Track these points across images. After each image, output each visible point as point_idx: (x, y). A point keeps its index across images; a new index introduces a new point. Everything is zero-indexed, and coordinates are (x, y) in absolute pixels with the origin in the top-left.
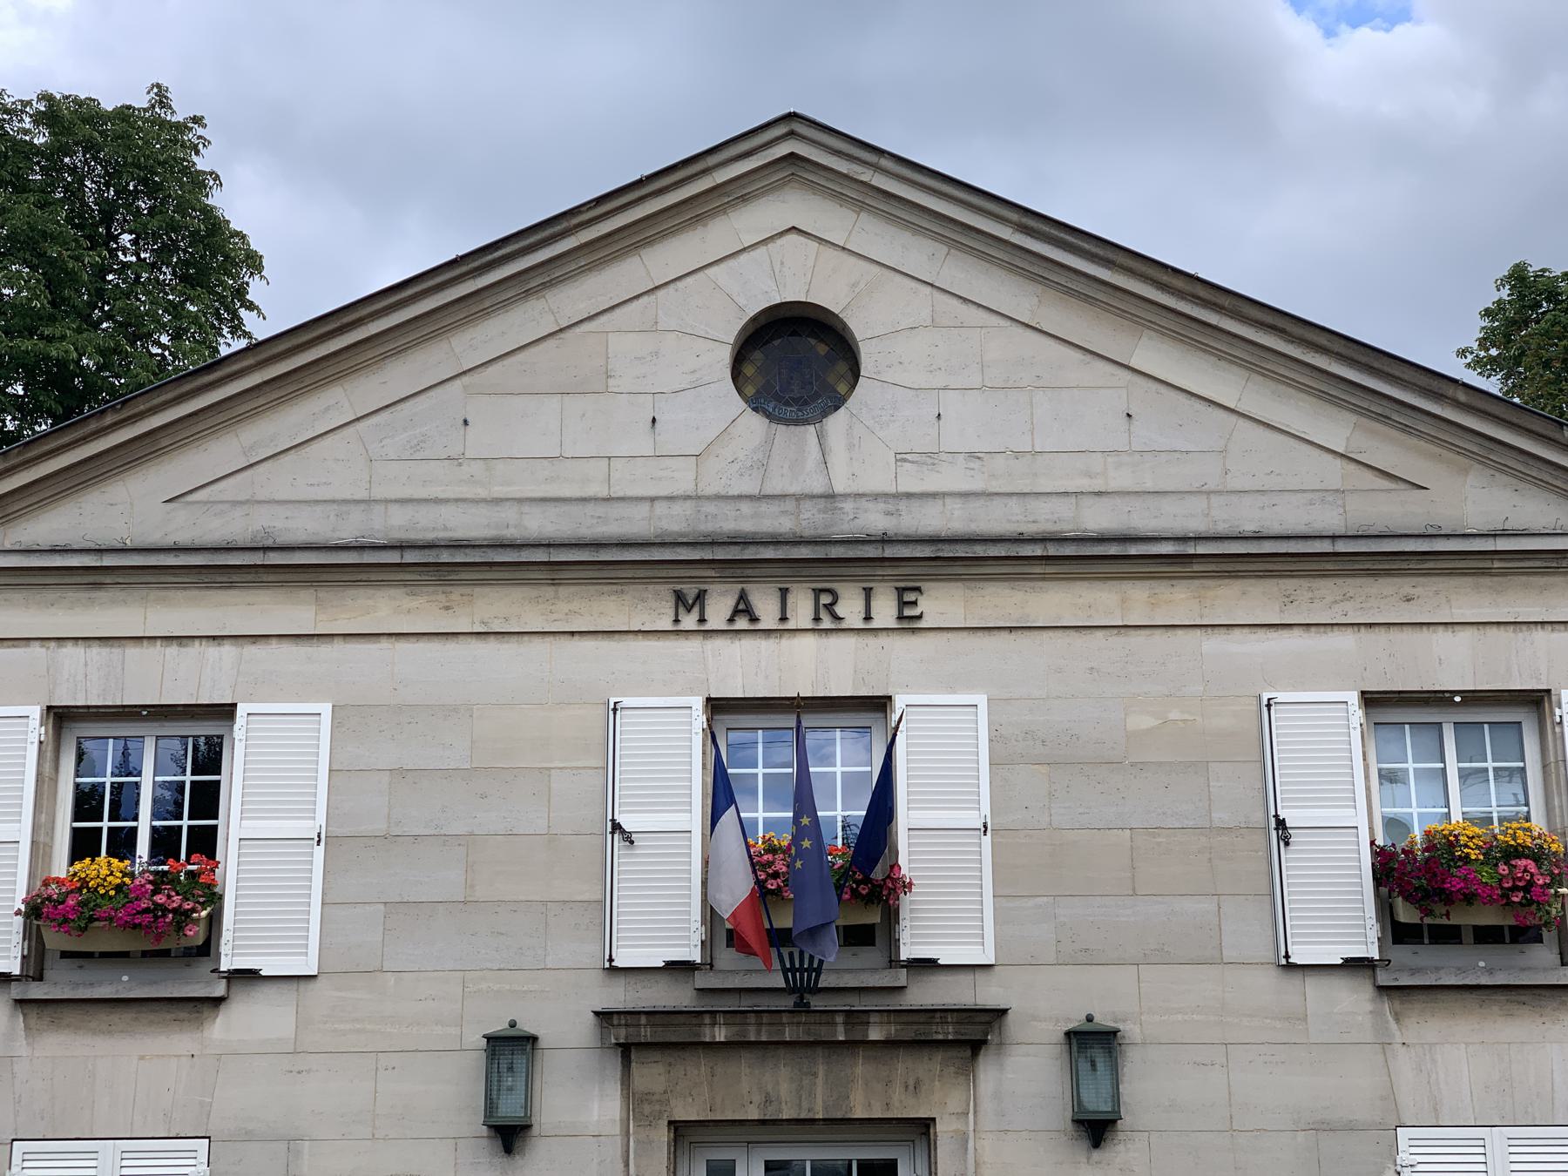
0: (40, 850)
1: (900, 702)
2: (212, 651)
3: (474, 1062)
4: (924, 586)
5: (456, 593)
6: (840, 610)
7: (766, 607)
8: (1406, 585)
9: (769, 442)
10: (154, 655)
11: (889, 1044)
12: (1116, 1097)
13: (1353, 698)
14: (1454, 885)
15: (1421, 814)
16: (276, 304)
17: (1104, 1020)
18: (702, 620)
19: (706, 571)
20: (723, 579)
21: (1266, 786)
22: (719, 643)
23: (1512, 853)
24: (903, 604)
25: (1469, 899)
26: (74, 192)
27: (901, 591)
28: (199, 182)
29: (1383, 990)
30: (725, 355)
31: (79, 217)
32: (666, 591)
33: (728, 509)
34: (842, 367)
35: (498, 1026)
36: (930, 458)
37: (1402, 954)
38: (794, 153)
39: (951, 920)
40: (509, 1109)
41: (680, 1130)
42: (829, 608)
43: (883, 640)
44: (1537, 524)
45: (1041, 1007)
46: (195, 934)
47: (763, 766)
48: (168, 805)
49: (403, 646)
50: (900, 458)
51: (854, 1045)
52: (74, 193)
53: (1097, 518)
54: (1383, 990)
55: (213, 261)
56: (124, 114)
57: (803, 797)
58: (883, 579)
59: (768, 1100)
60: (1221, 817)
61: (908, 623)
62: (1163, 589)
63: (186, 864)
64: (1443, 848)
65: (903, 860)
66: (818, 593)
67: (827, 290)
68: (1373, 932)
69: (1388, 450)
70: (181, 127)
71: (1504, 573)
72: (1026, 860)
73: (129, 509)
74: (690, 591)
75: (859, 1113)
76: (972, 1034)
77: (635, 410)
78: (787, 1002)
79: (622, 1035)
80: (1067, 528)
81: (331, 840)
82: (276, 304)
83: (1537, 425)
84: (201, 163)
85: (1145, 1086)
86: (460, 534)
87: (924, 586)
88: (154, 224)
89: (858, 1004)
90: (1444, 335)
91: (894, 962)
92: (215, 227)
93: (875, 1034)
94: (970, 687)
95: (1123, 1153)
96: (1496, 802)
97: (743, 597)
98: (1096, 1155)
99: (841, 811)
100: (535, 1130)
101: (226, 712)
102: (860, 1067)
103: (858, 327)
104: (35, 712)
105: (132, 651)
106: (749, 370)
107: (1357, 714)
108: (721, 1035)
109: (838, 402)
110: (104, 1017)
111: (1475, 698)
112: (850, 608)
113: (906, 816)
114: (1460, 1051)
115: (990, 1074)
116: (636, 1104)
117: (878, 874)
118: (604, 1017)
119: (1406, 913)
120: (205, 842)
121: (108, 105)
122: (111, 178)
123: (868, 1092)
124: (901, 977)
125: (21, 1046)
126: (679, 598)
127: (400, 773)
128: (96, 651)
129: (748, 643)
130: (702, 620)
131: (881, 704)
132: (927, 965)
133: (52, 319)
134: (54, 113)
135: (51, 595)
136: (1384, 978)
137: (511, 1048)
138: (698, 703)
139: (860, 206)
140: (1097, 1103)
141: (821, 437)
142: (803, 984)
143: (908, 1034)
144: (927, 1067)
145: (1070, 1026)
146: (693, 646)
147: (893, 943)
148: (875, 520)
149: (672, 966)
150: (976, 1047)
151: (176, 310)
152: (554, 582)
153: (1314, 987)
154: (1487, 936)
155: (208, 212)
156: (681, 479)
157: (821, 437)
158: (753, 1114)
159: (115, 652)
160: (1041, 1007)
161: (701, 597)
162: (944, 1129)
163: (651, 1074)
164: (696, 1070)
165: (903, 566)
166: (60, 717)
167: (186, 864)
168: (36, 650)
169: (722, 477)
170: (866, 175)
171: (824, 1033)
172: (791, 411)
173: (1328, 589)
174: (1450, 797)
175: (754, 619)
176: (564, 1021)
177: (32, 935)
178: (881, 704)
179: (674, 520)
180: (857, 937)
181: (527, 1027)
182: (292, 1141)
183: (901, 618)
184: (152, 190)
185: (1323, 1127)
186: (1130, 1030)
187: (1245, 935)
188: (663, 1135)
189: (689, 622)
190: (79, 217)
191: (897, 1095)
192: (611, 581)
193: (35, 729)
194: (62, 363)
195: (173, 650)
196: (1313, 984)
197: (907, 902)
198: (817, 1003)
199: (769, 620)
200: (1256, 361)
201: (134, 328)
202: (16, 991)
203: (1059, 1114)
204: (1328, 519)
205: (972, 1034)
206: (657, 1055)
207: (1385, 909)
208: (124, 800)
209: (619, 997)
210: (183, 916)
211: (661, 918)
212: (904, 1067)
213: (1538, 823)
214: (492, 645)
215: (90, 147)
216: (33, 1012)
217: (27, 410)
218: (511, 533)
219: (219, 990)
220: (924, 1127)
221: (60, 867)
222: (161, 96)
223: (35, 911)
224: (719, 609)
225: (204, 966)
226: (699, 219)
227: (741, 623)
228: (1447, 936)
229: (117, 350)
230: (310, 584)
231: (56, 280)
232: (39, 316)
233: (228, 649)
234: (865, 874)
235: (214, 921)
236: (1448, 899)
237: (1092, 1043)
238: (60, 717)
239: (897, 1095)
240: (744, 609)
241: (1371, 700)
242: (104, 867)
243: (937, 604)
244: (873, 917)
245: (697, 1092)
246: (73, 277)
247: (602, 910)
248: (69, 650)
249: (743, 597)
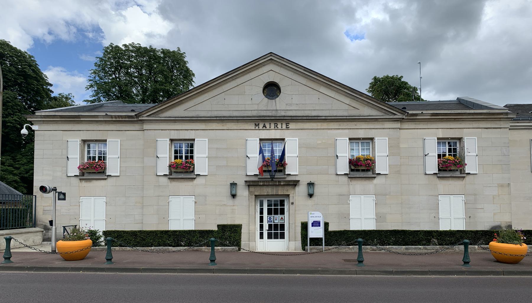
0: (170, 158)
1: (286, 139)
2: (191, 131)
3: (229, 186)
5: (224, 123)
7: (268, 126)
9: (268, 102)
10: (184, 132)
11: (284, 185)
12: (314, 191)
13: (348, 139)
14: (359, 164)
17: (312, 182)
19: (259, 121)
21: (335, 151)
22: (261, 131)
23: (367, 160)
25: (361, 166)
28: (185, 63)
29: (349, 177)
30: (262, 89)
31: (168, 67)
32: (254, 124)
33: (262, 112)
34: (278, 91)
35: (232, 182)
36: (291, 105)
37: (352, 173)
38: (271, 58)
39: (293, 168)
40: (234, 193)
43: (284, 131)
44: (374, 114)
45: (304, 180)
46: (191, 169)
48: (187, 152)
49: (217, 131)
50: (287, 105)
52: (167, 64)
54: (349, 177)
56: (174, 52)
60: (329, 155)
61: (287, 128)
62: (323, 123)
63: (189, 160)
64: (358, 159)
65: (286, 161)
67: (276, 79)
68: (348, 170)
70: (182, 54)
71: (369, 121)
72: (302, 161)
76: (295, 184)
78: (270, 180)
79: (248, 184)
80: (310, 115)
81: (209, 157)
83: (375, 100)
84: (185, 60)
85: (317, 190)
86: (225, 115)
88: (179, 69)
89: (280, 180)
91: (285, 174)
93: (282, 184)
94: (296, 137)
96: (365, 153)
99: (278, 154)
101: (194, 140)
102: (280, 188)
103: (281, 85)
104: (168, 140)
105: (181, 131)
106: (265, 91)
107: (348, 141)
109: (278, 96)
110: (180, 180)
111: (364, 139)
112: (279, 126)
113: (287, 155)
115: (297, 188)
116: (250, 193)
117: (283, 163)
118: (246, 181)
119: (353, 168)
120: (192, 157)
121: (171, 50)
122: (173, 62)
124: (286, 176)
126: (255, 124)
128: (176, 131)
129: (265, 131)
131: (283, 140)
132: (290, 175)
133: (166, 83)
135: (169, 123)
136: (349, 176)
138: (258, 139)
139: (281, 67)
140: (311, 192)
141: (275, 102)
142: (272, 178)
144: (289, 188)
146: (258, 131)
147: (285, 172)
148: (283, 114)
149: (255, 175)
150: (295, 185)
153: (340, 177)
154: (363, 170)
155: (187, 67)
156: (256, 107)
157: (275, 102)
159: (178, 131)
160: (304, 180)
161: (258, 124)
163: (252, 189)
164: (258, 188)
165: (286, 120)
166: (172, 140)
167: (189, 160)
168: (168, 131)
169: (262, 107)
170: (282, 62)
171: (275, 184)
172: (271, 98)
174: (360, 152)
176: (241, 182)
177: (170, 169)
179: (255, 113)
180: (280, 171)
181: (235, 182)
184: (179, 64)
185: (340, 195)
187: (332, 171)
188: (254, 197)
189: (257, 128)
190: (168, 67)
191: (285, 191)
192: (245, 122)
193: (168, 142)
194: (168, 90)
195: (186, 131)
196: (340, 177)
197: (287, 166)
198: (274, 180)
199: (268, 128)
202: (168, 177)
203: (306, 194)
205: (295, 184)
207: (350, 167)
208: (181, 152)
209: (248, 179)
212: (286, 188)
213: (371, 156)
214: (229, 131)
215: (169, 57)
217: (163, 97)
218: (232, 115)
219: (195, 177)
220: (288, 195)
221: (173, 160)
223: (170, 166)
224: (261, 126)
225: (193, 174)
226: (257, 68)
227: (264, 128)
228: (358, 170)
229: (175, 88)
231: (166, 77)
232: (164, 83)
233: (193, 131)
234: (281, 162)
235: (194, 168)
236: (358, 166)
237: (311, 185)
238: (172, 140)
239: (285, 191)
240: (264, 126)
241: (350, 139)
242: (179, 161)
243: (292, 125)
244: (282, 168)
246: (168, 77)
247: (245, 167)
248: (172, 131)
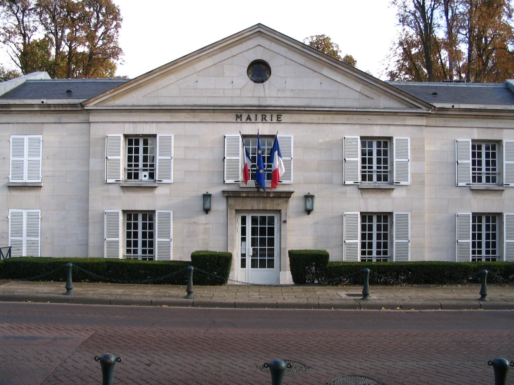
4: (282, 114)
6: (266, 119)
8: (369, 117)
12: (313, 206)
18: (241, 120)
20: (245, 113)
24: (278, 118)
27: (278, 115)
35: (205, 193)
38: (260, 31)
40: (207, 206)
42: (265, 118)
43: (274, 124)
49: (187, 124)
51: (268, 197)
58: (275, 113)
59: (252, 206)
61: (279, 121)
66: (262, 115)
69: (367, 91)
74: (239, 114)
75: (268, 209)
76: (288, 195)
79: (226, 195)
87: (282, 114)
93: (271, 195)
97: (249, 116)
98: (309, 216)
100: (212, 210)
102: (269, 200)
108: (244, 195)
112: (268, 118)
123: (269, 205)
125: (122, 194)
126: (237, 116)
127: (186, 147)
130: (241, 120)
139: (272, 41)
140: (309, 207)
143: (277, 195)
144: (280, 201)
145: (305, 194)
152: (214, 113)
158: (250, 208)
161: (241, 116)
162: (283, 212)
163: (232, 201)
164: (240, 201)
171: (262, 195)
175: (251, 120)
183: (278, 120)
186: (316, 195)
187: (336, 179)
188: (234, 212)
189: (239, 120)
195: (145, 125)
199: (253, 120)
203: (302, 209)
206: (233, 198)
209: (225, 188)
216: (124, 188)
220: (279, 211)
227: (248, 121)
230: (169, 112)
237: (309, 197)
240: (249, 118)
243: (285, 118)
245: (240, 205)
249: (249, 116)
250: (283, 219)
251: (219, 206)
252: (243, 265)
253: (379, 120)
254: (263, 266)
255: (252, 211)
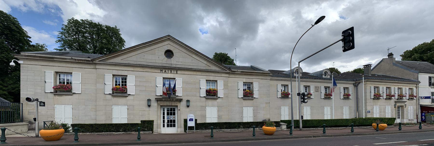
0: (113, 85)
7: (167, 71)
15: (208, 88)
16: (127, 45)
19: (163, 68)
26: (109, 34)
30: (164, 53)
36: (178, 62)
39: (179, 93)
40: (149, 104)
41: (161, 106)
45: (185, 99)
46: (125, 91)
47: (167, 83)
48: (122, 82)
53: (190, 67)
55: (121, 41)
57: (170, 84)
61: (177, 73)
63: (124, 86)
69: (209, 64)
72: (184, 89)
73: (118, 60)
76: (180, 100)
77: (157, 56)
81: (135, 85)
82: (127, 45)
85: (191, 104)
90: (211, 57)
92: (121, 38)
95: (189, 108)
99: (172, 86)
102: (173, 102)
111: (213, 81)
112: (173, 72)
113: (176, 86)
114: (210, 102)
115: (181, 103)
116: (158, 104)
120: (126, 85)
131: (175, 79)
134: (106, 27)
137: (149, 100)
140: (188, 105)
142: (169, 97)
144: (177, 102)
148: (175, 66)
151: (118, 45)
154: (212, 95)
160: (185, 99)
163: (159, 102)
164: (162, 102)
165: (177, 69)
166: (114, 75)
167: (124, 86)
173: (204, 73)
176: (153, 99)
178: (175, 79)
179: (160, 65)
182: (134, 106)
187: (198, 95)
193: (112, 76)
200: (201, 57)
201: (115, 46)
204: (204, 68)
205: (180, 100)
209: (157, 97)
210: (124, 90)
211: (160, 92)
212: (176, 102)
221: (114, 86)
222: (116, 27)
224: (164, 71)
228: (210, 95)
235: (127, 91)
237: (188, 101)
240: (165, 71)
241: (206, 80)
242: (118, 86)
243: (179, 72)
245: (162, 103)
247: (155, 91)
250: (179, 109)
251: (154, 104)
252: (164, 126)
253: (213, 74)
254: (171, 126)
255: (167, 106)
